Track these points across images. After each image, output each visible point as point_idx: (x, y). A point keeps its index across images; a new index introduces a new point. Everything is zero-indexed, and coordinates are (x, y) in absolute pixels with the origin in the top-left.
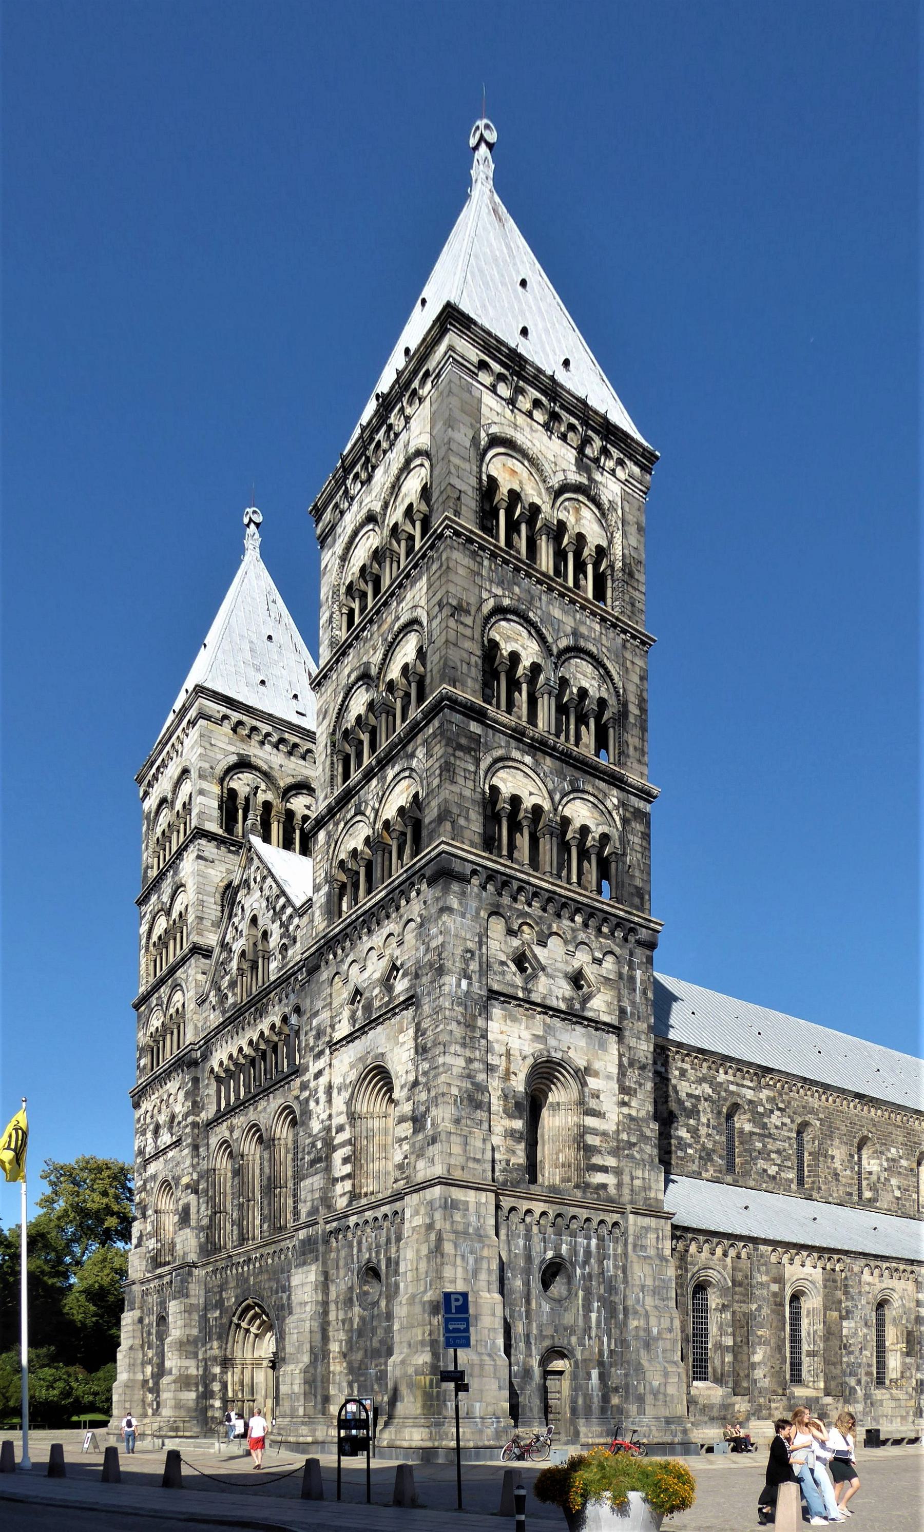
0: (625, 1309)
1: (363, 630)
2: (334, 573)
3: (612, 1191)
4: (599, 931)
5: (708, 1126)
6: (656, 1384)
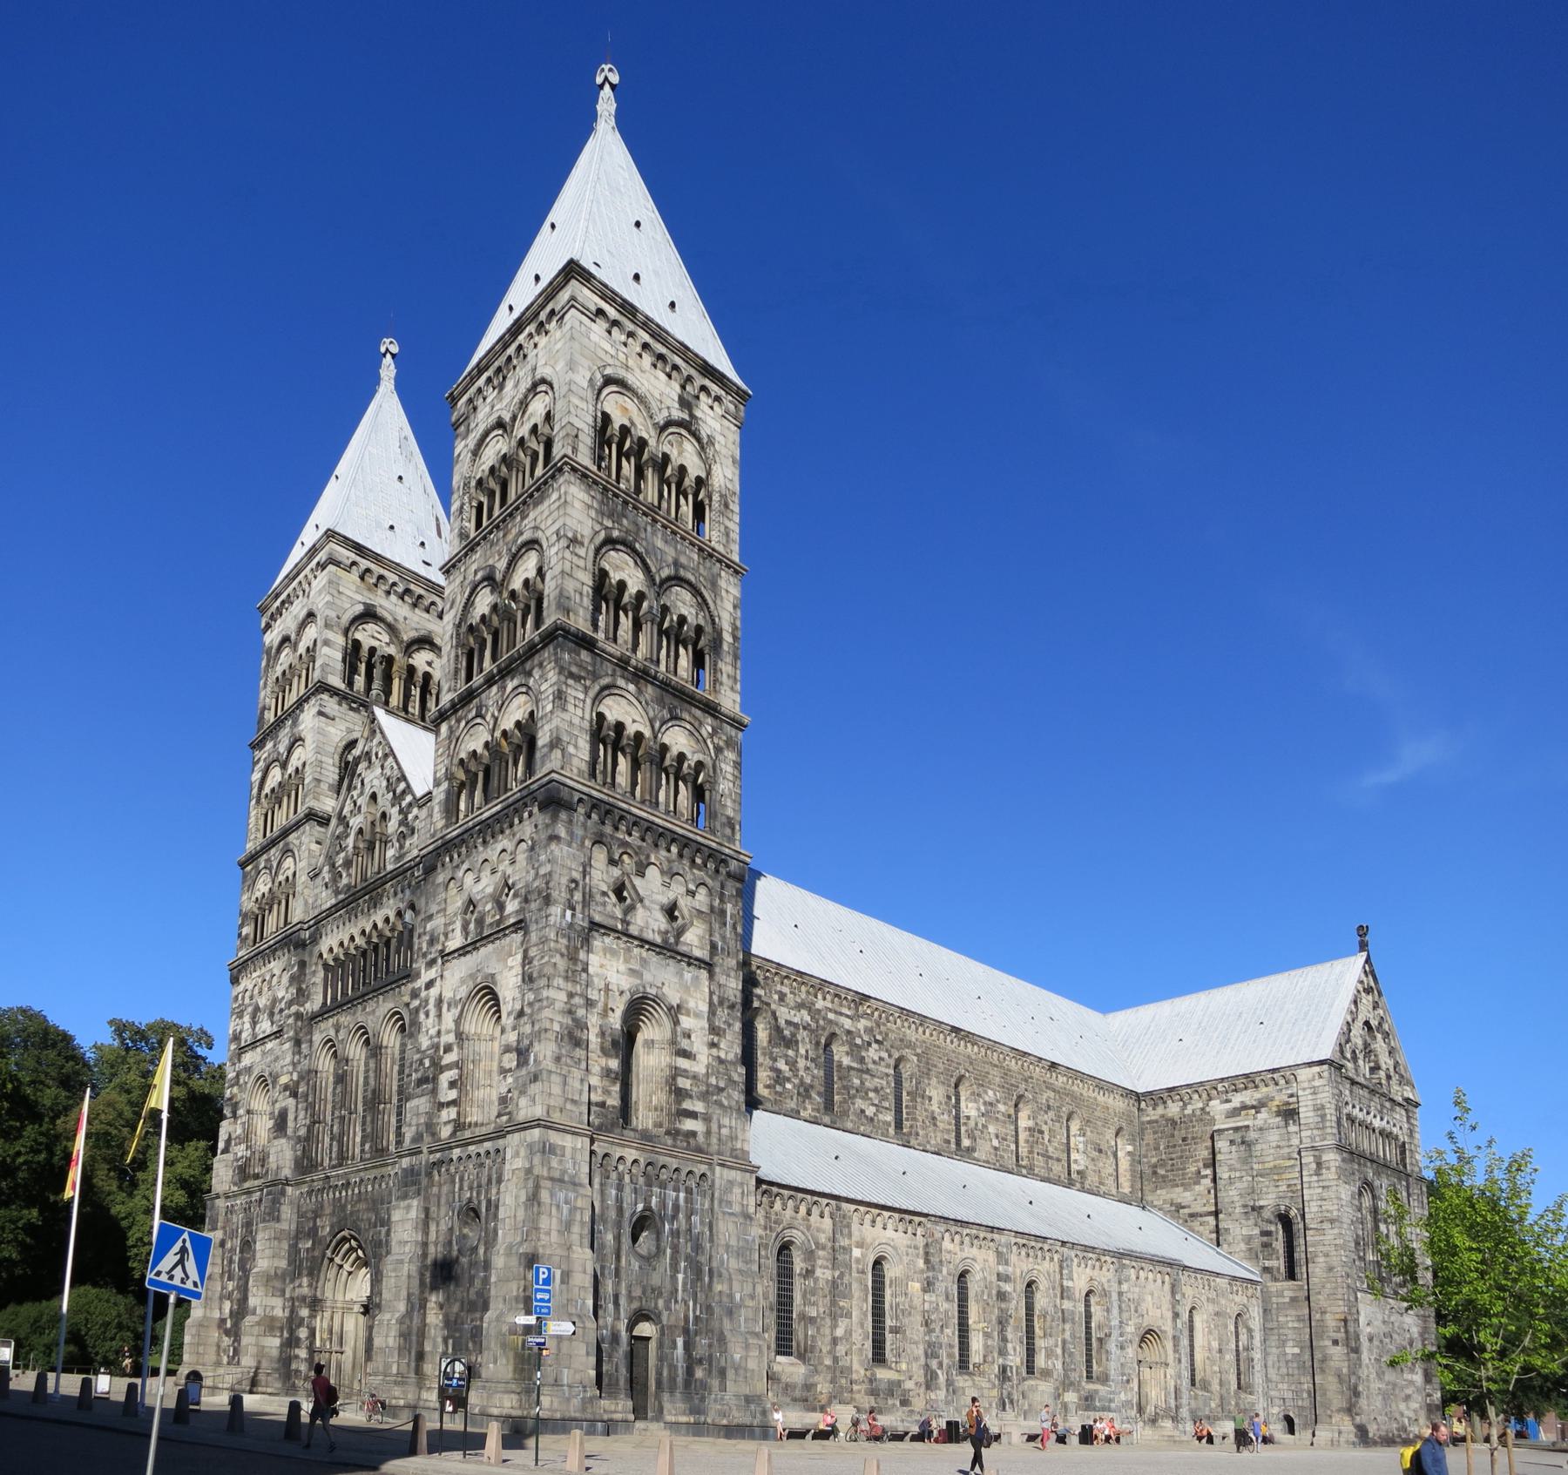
0: (710, 1270)
1: (491, 532)
2: (466, 466)
3: (701, 1139)
5: (807, 1058)
6: (737, 1357)
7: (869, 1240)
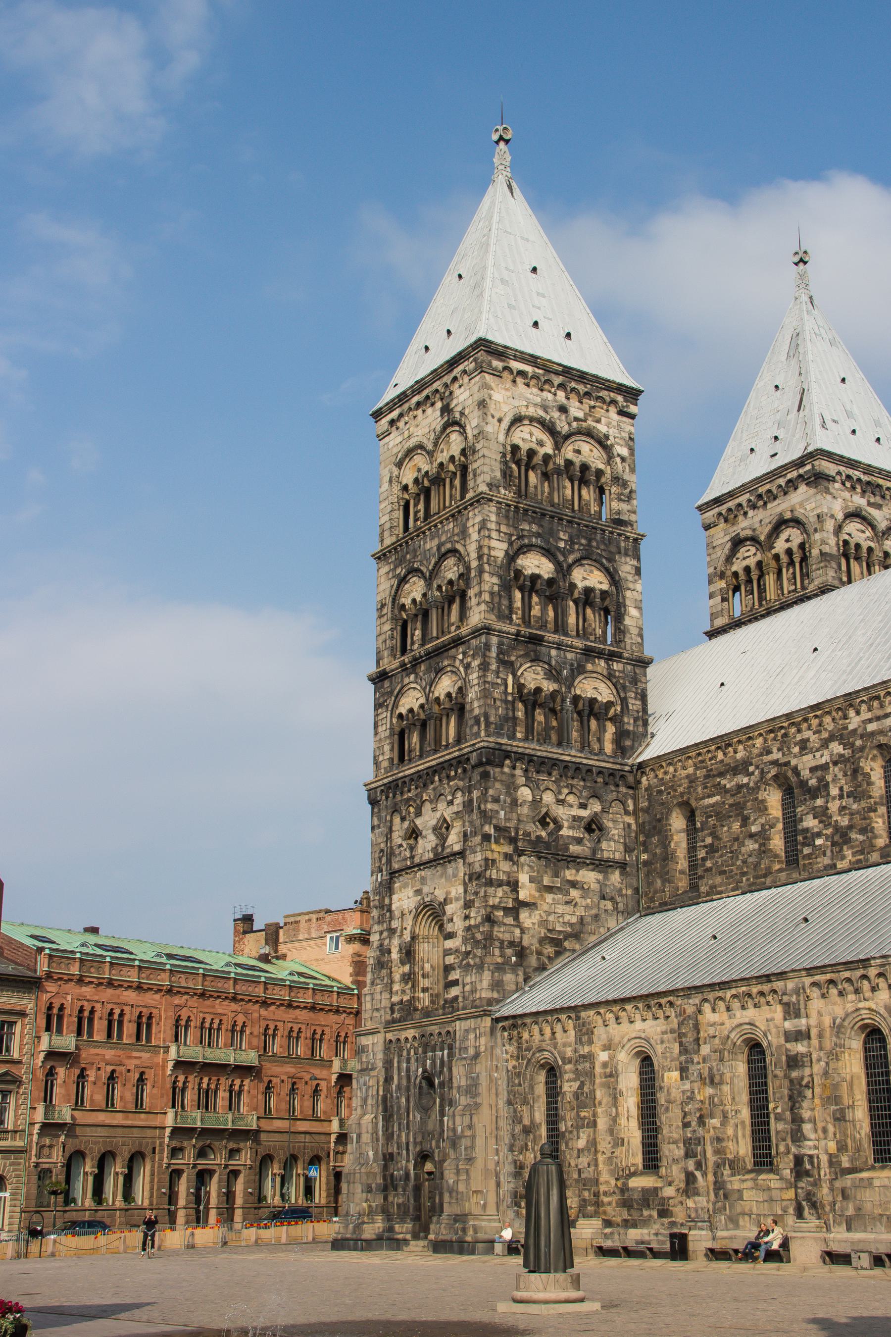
4: (448, 777)
6: (451, 1181)
7: (616, 1040)
